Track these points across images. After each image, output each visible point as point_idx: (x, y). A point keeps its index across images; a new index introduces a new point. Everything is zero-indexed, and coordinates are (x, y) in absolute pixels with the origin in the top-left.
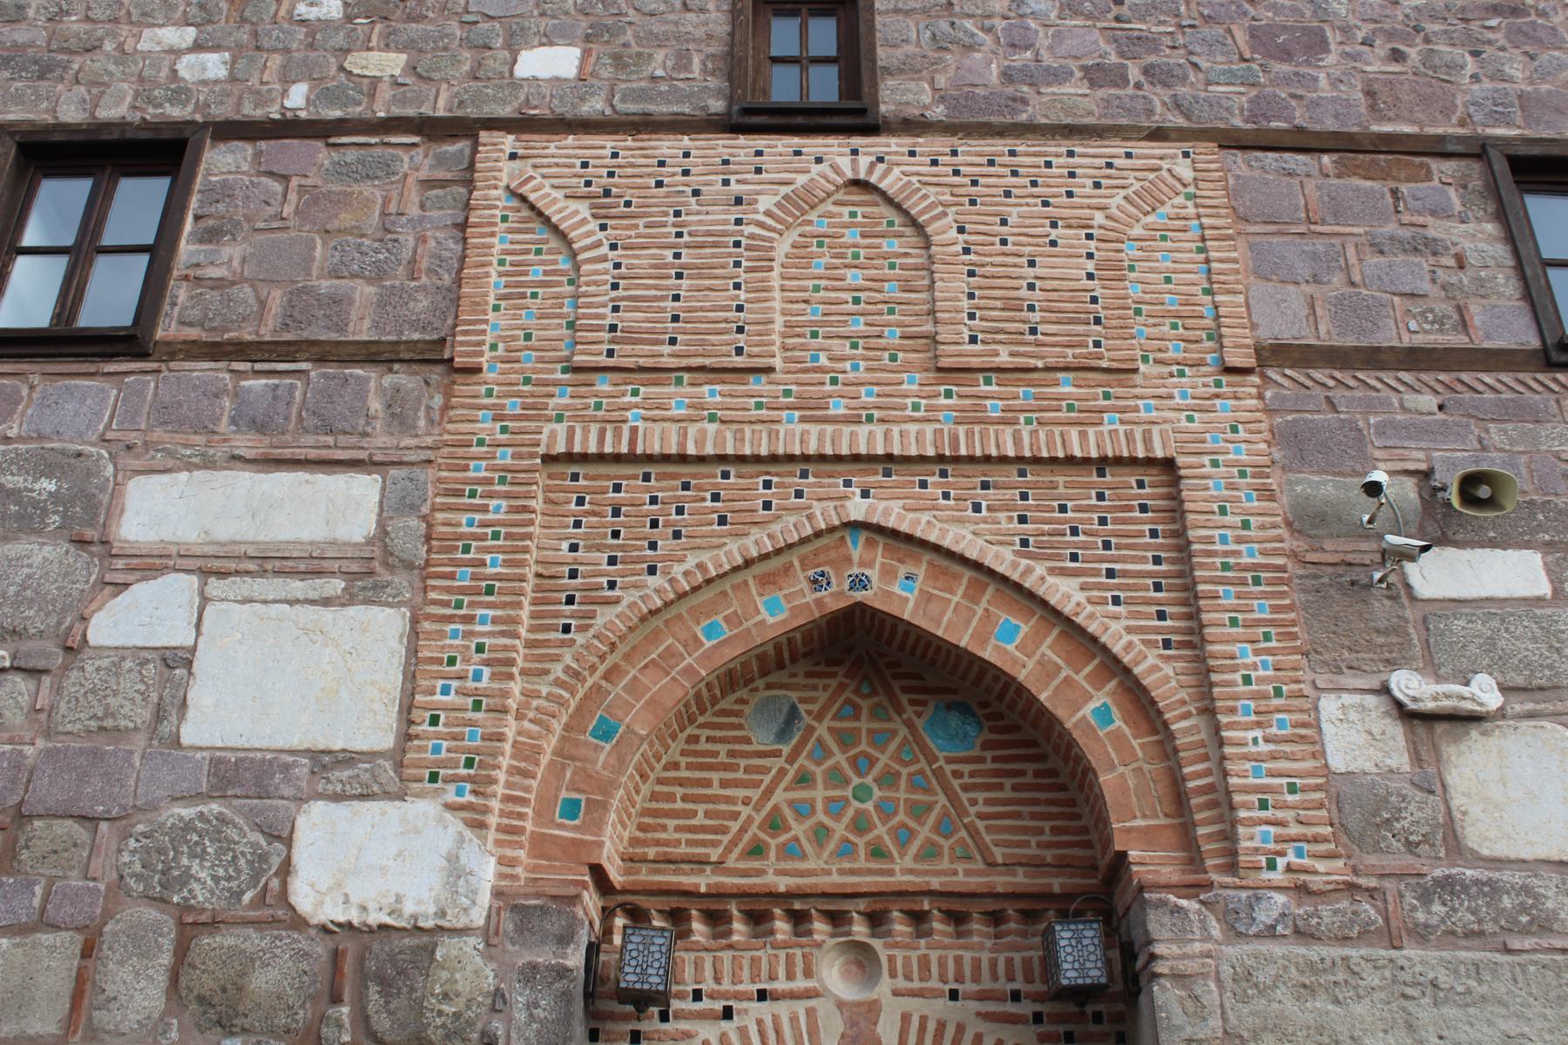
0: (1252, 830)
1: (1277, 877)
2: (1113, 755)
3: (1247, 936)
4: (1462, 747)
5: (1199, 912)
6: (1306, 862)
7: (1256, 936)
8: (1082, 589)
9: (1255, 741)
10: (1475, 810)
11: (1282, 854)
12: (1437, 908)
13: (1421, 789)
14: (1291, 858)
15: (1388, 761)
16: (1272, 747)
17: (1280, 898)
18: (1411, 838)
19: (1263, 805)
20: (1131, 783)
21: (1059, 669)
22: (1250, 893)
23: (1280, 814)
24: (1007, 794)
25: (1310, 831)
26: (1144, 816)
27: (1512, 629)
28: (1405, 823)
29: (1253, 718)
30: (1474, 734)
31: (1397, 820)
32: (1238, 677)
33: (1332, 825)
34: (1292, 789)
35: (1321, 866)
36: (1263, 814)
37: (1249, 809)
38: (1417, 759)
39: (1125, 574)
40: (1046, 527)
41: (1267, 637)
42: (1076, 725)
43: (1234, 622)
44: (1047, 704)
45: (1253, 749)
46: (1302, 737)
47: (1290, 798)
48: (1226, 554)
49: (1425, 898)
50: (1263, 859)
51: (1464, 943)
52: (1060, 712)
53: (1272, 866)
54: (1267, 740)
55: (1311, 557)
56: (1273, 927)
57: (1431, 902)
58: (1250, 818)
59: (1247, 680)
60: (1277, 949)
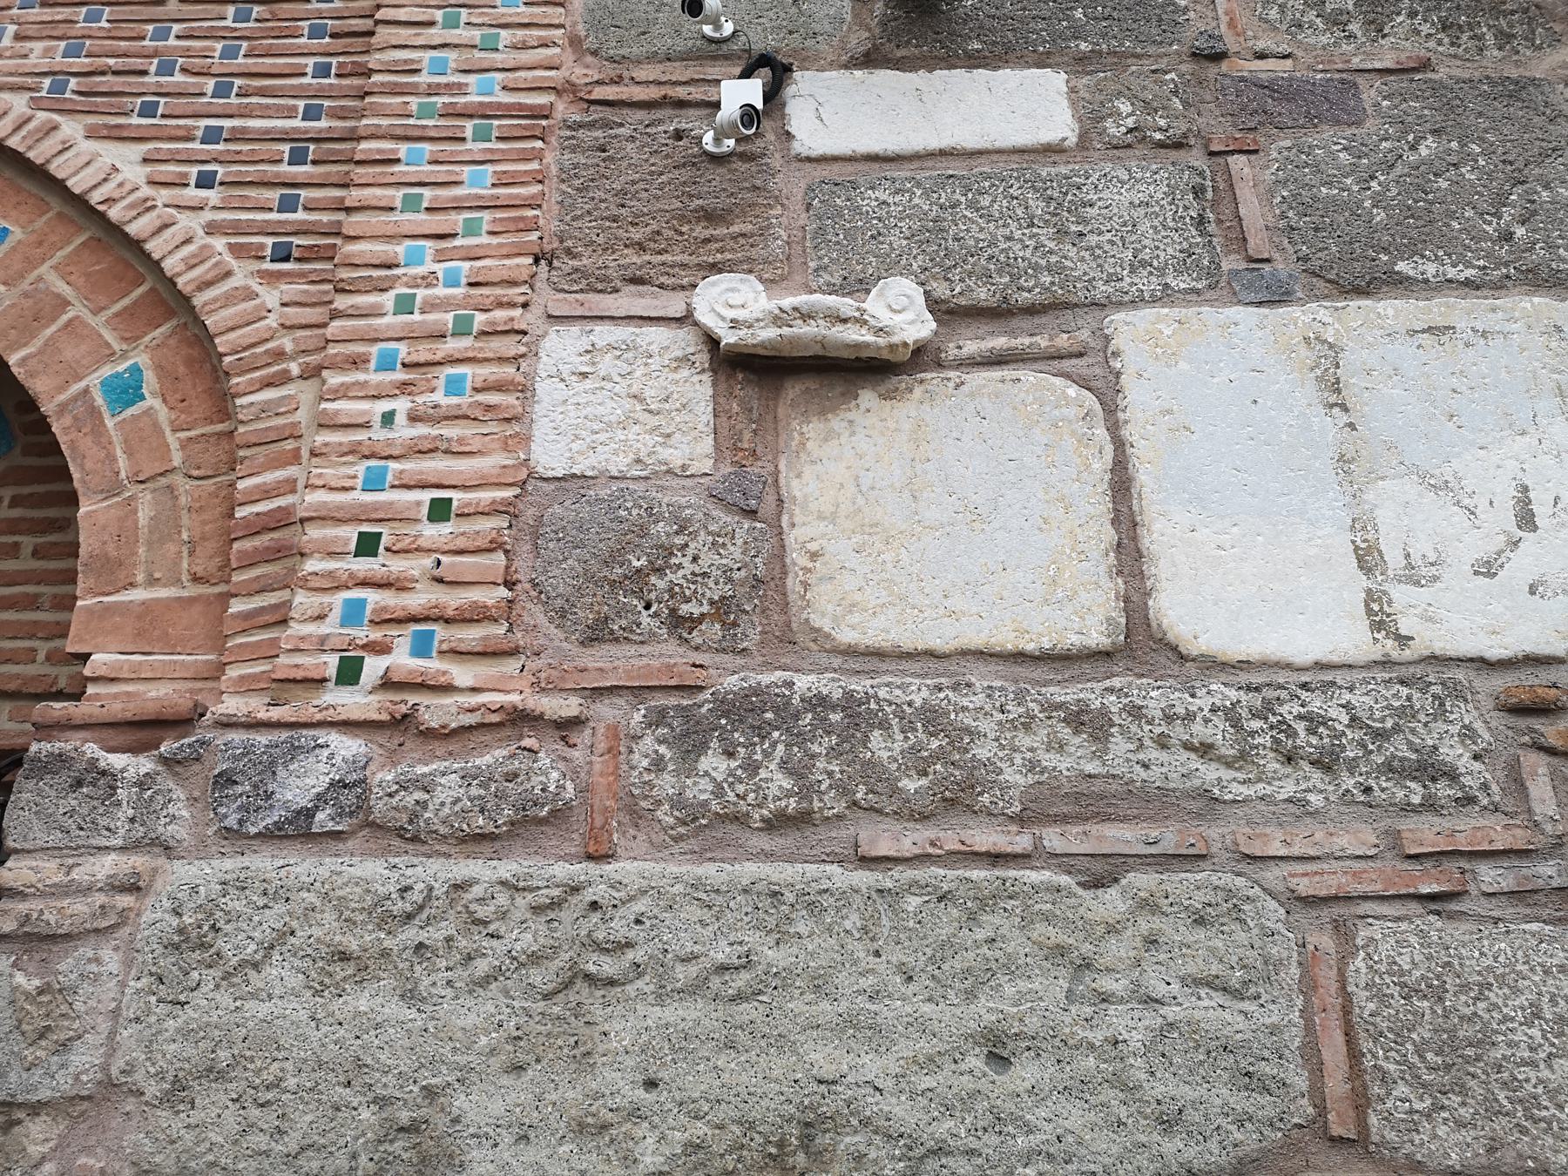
0: (326, 599)
1: (354, 701)
2: (122, 463)
3: (248, 837)
4: (836, 423)
5: (142, 783)
6: (433, 665)
7: (266, 836)
8: (145, 160)
9: (388, 418)
10: (839, 549)
11: (381, 649)
12: (713, 763)
13: (731, 507)
14: (402, 659)
15: (665, 453)
16: (422, 430)
17: (347, 747)
18: (685, 609)
19: (368, 546)
20: (144, 516)
21: (65, 304)
22: (285, 735)
23: (397, 565)
24: (26, 563)
25: (453, 600)
26: (152, 582)
27: (985, 201)
28: (677, 577)
29: (400, 375)
30: (867, 397)
31: (659, 571)
32: (388, 300)
33: (510, 584)
34: (440, 511)
35: (463, 675)
36: (363, 566)
37: (332, 554)
38: (727, 444)
39: (237, 136)
40: (111, 61)
41: (471, 229)
42: (62, 409)
43: (411, 204)
44: (15, 370)
45: (378, 434)
46: (489, 408)
47: (433, 533)
48: (434, 90)
49: (691, 743)
50: (333, 661)
51: (763, 842)
52: (39, 386)
53: (349, 673)
54: (414, 418)
55: (599, 93)
56: (309, 814)
57: (702, 748)
58: (330, 574)
59: (405, 305)
60: (303, 865)
